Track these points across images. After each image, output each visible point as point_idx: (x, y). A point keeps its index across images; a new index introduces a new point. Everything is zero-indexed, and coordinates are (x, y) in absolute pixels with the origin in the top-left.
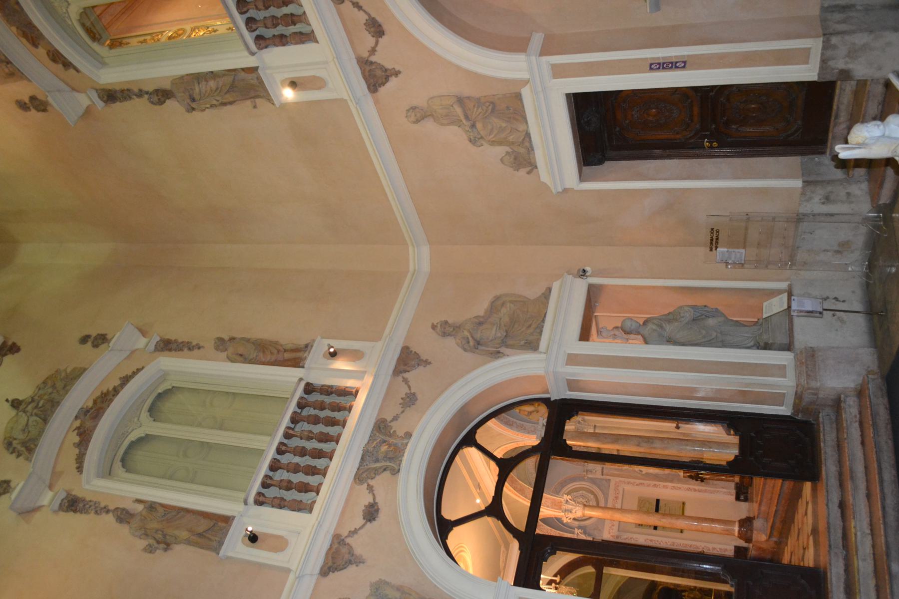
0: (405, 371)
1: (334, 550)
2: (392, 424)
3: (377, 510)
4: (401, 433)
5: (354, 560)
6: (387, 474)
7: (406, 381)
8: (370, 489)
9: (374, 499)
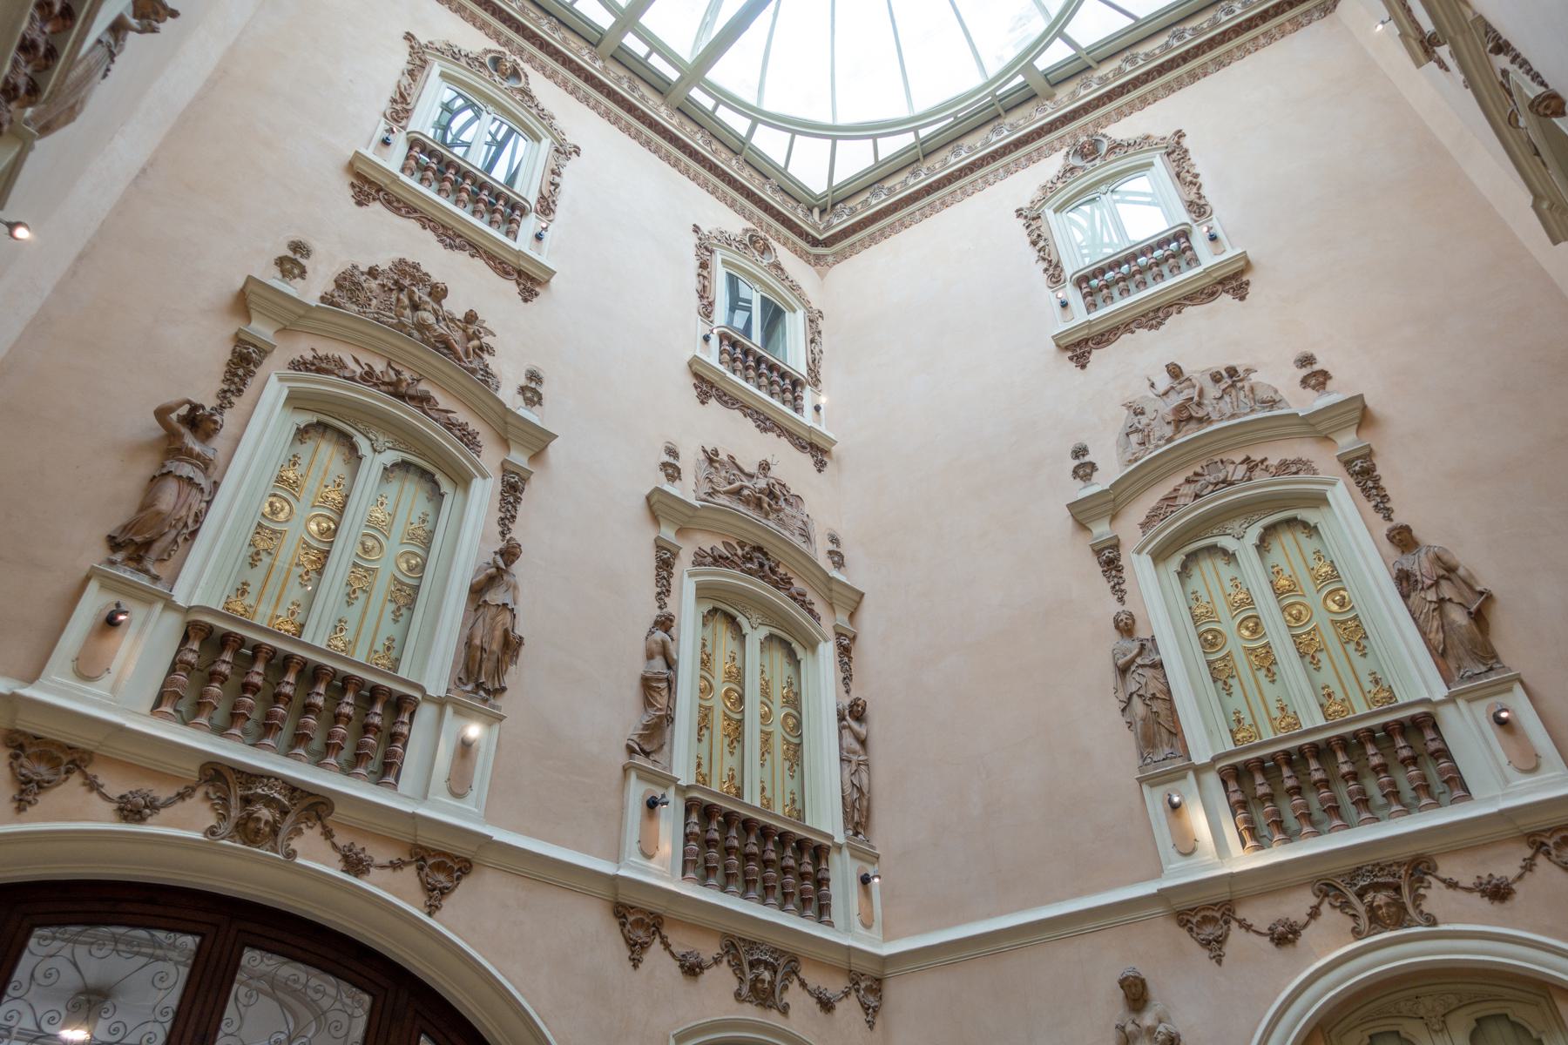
0: (1548, 854)
1: (1209, 913)
3: (1293, 942)
4: (1426, 907)
5: (1214, 947)
7: (1529, 866)
8: (1314, 913)
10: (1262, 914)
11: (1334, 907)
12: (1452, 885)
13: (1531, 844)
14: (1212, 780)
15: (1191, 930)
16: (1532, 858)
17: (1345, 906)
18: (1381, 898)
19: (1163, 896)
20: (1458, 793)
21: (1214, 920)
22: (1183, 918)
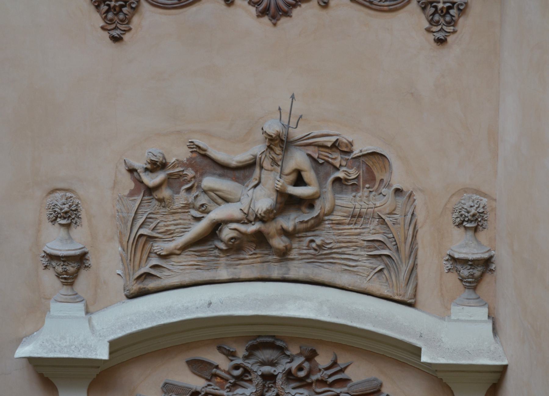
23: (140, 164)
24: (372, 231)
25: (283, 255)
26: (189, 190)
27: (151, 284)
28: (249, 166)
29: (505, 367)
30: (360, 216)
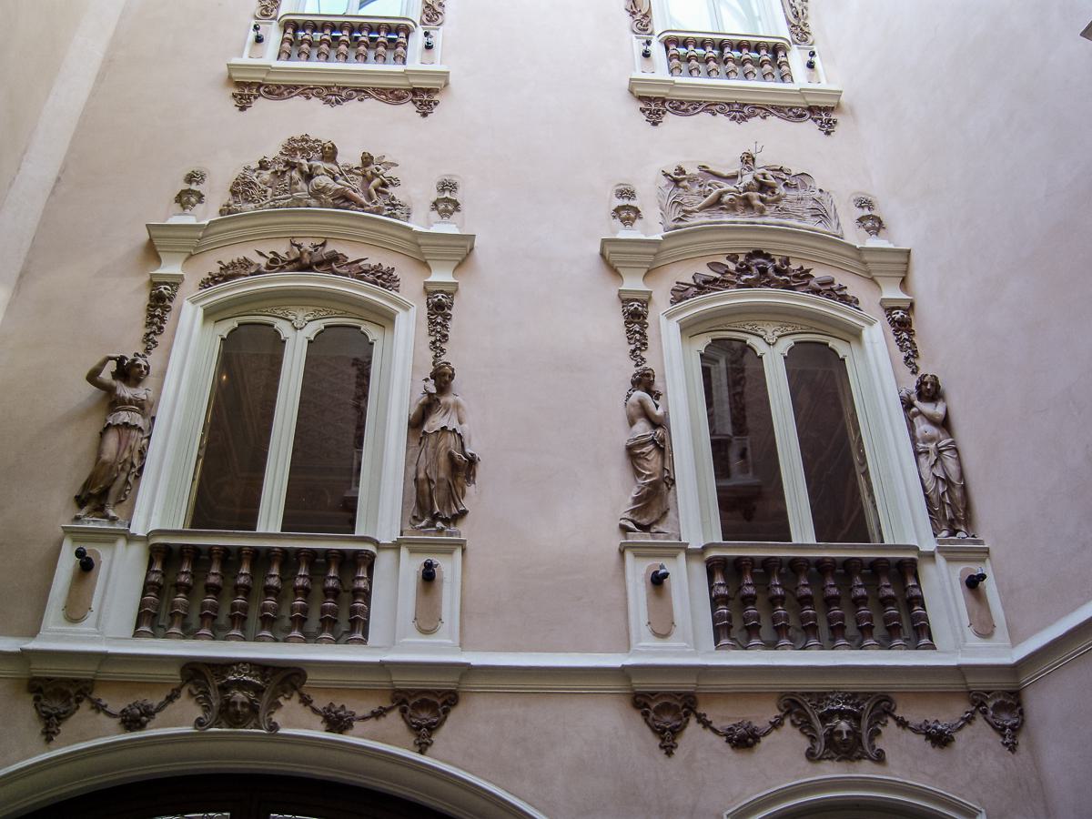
0: (985, 712)
2: (892, 723)
5: (668, 739)
6: (804, 743)
9: (765, 735)
10: (722, 715)
11: (792, 722)
12: (902, 723)
13: (973, 702)
14: (700, 570)
15: (645, 714)
16: (972, 712)
17: (805, 726)
18: (844, 725)
19: (624, 672)
20: (925, 641)
21: (675, 710)
22: (640, 702)
23: (671, 171)
24: (811, 204)
25: (762, 212)
26: (700, 186)
27: (681, 224)
28: (735, 177)
29: (909, 251)
30: (802, 199)
